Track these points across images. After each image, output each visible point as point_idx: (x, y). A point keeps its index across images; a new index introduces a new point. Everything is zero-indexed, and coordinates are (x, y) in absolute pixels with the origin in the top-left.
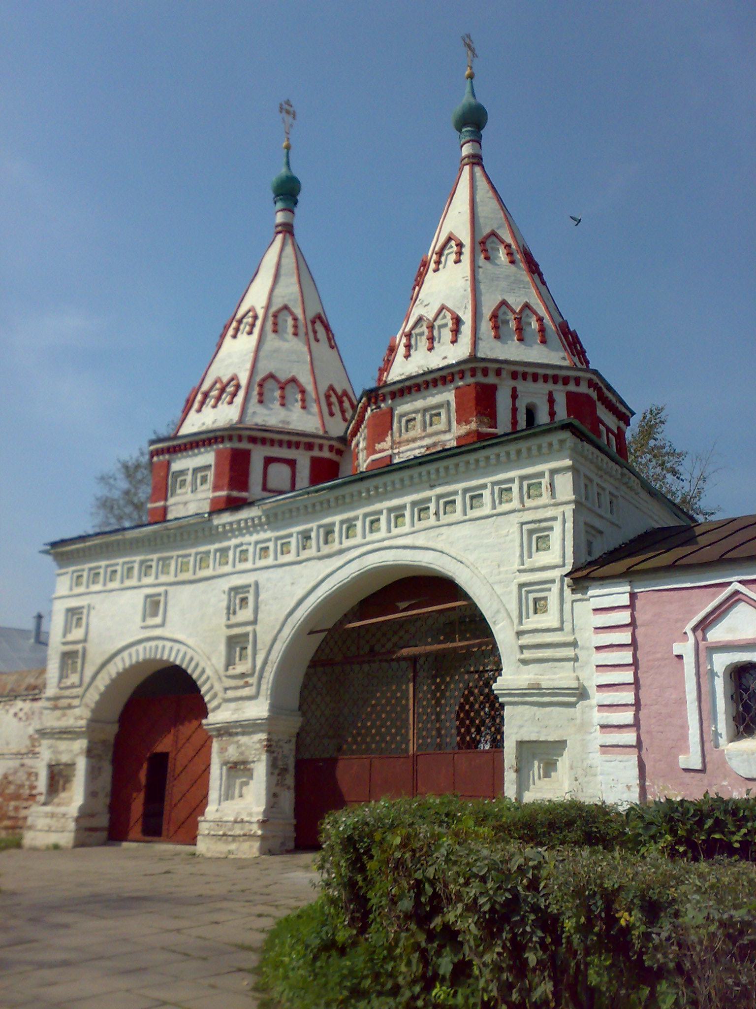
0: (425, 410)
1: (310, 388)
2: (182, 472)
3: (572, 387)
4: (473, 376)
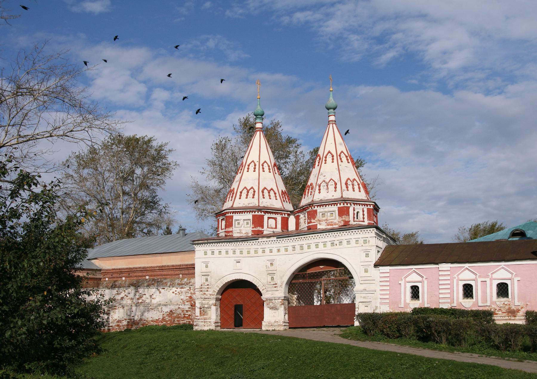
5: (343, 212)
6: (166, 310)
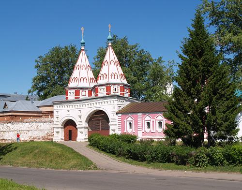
5: (108, 89)
6: (46, 132)
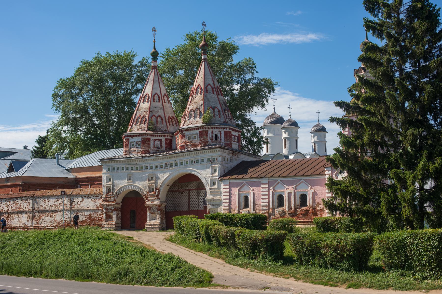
0: (193, 134)
1: (164, 119)
2: (132, 142)
3: (225, 130)
4: (203, 129)
6: (87, 213)
